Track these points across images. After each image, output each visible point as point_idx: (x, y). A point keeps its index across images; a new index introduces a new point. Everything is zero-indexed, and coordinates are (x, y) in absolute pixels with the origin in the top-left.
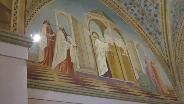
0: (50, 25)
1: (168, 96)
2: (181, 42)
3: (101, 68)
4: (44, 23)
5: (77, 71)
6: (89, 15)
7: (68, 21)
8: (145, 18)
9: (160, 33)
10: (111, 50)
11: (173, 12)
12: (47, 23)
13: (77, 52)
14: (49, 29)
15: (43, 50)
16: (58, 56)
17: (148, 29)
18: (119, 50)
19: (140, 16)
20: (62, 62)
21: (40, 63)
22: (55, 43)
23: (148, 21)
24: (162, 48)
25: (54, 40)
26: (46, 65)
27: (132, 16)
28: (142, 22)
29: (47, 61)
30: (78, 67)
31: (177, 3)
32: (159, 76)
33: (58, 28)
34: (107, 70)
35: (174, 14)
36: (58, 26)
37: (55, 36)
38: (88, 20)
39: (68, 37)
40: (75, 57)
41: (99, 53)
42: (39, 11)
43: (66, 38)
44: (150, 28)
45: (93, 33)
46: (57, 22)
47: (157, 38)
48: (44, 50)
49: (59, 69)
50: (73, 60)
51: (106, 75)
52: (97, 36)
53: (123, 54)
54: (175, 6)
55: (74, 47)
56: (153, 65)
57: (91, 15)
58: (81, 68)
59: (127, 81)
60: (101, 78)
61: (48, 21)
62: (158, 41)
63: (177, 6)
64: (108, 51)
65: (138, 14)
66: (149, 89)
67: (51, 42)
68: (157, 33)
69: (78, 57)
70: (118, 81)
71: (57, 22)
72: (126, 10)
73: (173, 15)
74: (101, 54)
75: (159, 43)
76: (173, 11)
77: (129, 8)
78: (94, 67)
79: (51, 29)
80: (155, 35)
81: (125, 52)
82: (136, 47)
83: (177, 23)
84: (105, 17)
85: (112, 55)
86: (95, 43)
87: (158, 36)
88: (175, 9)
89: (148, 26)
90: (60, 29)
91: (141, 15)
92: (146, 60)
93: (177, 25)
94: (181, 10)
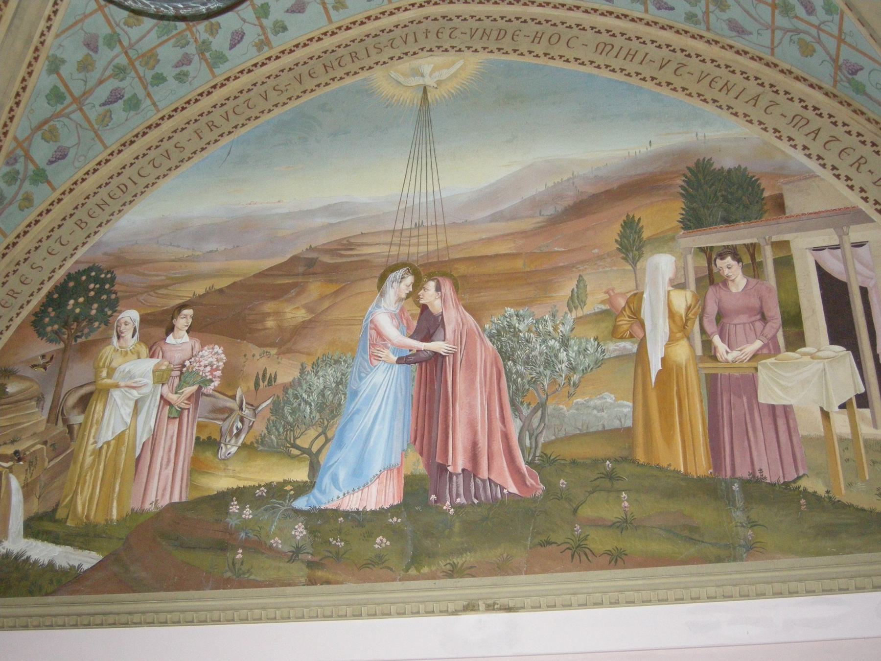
2: (24, 269)
11: (64, 71)
31: (113, 40)
35: (62, 89)
54: (91, 44)
63: (105, 56)
73: (55, 87)
76: (63, 61)
83: (61, 155)
88: (85, 66)
93: (51, 162)
94: (115, 96)
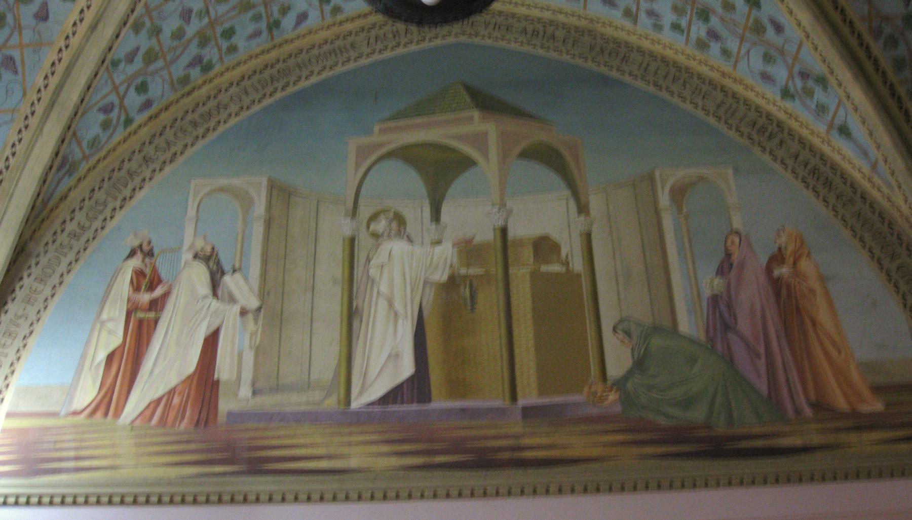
0: (153, 255)
1: (871, 423)
3: (374, 371)
4: (132, 254)
5: (230, 414)
6: (376, 138)
7: (247, 203)
8: (724, 33)
9: (822, 81)
10: (463, 271)
12: (142, 250)
13: (254, 334)
14: (144, 276)
15: (99, 364)
16: (156, 372)
17: (766, 77)
18: (528, 254)
19: (699, 30)
20: (171, 393)
21: (75, 413)
22: (156, 321)
23: (742, 39)
24: (866, 154)
25: (156, 311)
26: (99, 415)
27: (667, 36)
28: (726, 53)
29: (107, 399)
30: (245, 391)
32: (823, 316)
33: (190, 256)
34: (407, 368)
36: (192, 246)
37: (166, 296)
38: (357, 169)
39: (227, 279)
40: (240, 355)
41: (382, 305)
42: (120, 215)
43: (215, 285)
44: (770, 69)
45: (374, 217)
46: (189, 230)
47: (821, 109)
48: (104, 363)
49: (150, 419)
50: (224, 369)
51: (393, 396)
52: (394, 225)
53: (544, 268)
55: (243, 312)
56: (783, 271)
57: (385, 138)
58: (255, 393)
59: (529, 397)
60: (360, 419)
61: (149, 243)
62: (838, 122)
64: (445, 278)
65: (684, 23)
66: (698, 414)
67: (140, 322)
68: (810, 83)
69: (258, 351)
70: (463, 410)
71: (189, 230)
72: (628, 24)
74: (391, 304)
75: (844, 131)
77: (634, 10)
78: (328, 375)
79: (155, 271)
80: (809, 93)
81: (564, 253)
82: (664, 200)
84: (476, 114)
85: (468, 294)
86: (372, 263)
87: (819, 95)
89: (756, 61)
90: (196, 256)
91: (700, 23)
92: (728, 255)
